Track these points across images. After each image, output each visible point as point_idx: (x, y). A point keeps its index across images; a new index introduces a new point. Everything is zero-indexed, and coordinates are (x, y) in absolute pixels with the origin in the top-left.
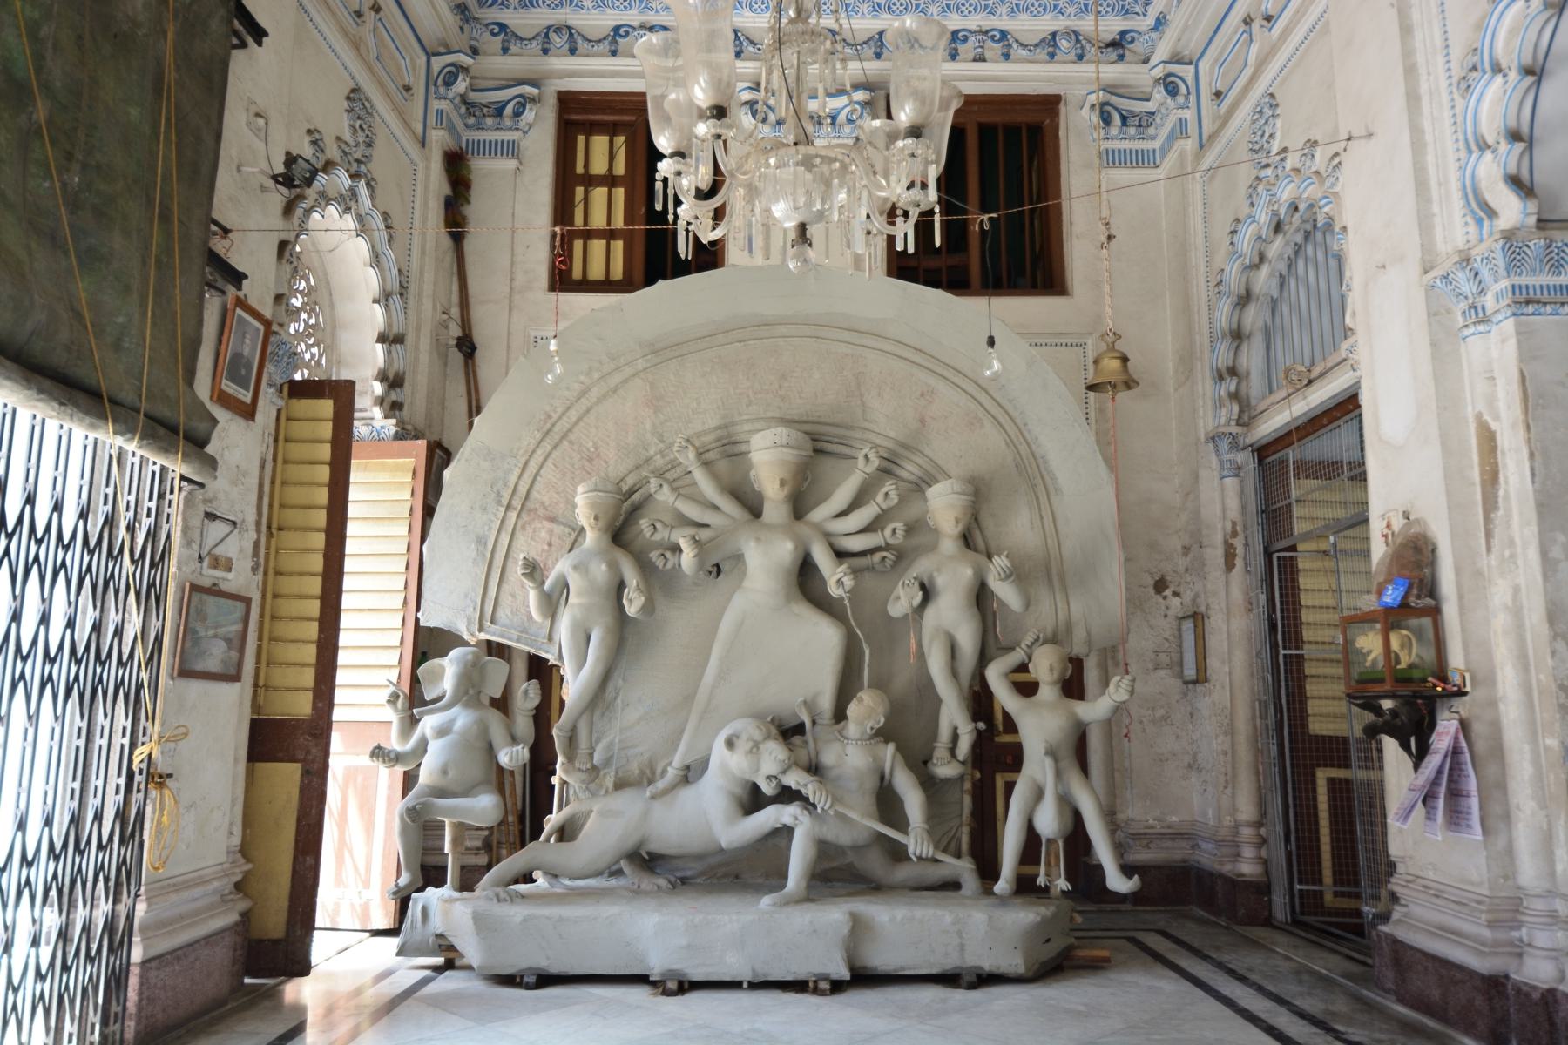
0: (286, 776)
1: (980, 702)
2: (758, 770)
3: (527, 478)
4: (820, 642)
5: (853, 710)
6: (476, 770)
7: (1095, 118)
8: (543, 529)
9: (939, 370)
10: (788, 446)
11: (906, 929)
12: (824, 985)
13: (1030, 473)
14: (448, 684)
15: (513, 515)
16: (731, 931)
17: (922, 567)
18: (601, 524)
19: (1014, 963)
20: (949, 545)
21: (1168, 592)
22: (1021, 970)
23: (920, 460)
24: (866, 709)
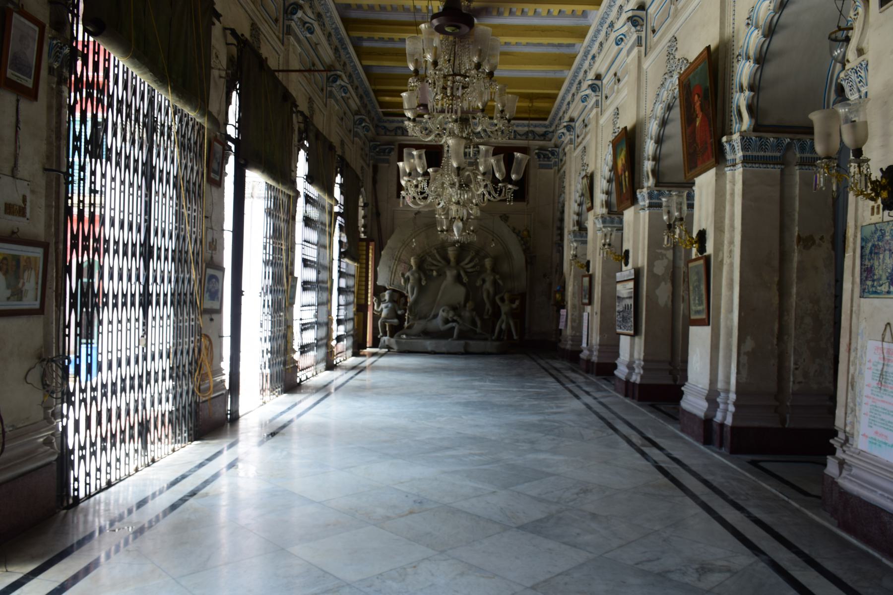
0: (361, 314)
1: (494, 304)
5: (468, 305)
8: (403, 265)
11: (474, 345)
14: (387, 297)
16: (443, 345)
20: (489, 272)
24: (470, 305)
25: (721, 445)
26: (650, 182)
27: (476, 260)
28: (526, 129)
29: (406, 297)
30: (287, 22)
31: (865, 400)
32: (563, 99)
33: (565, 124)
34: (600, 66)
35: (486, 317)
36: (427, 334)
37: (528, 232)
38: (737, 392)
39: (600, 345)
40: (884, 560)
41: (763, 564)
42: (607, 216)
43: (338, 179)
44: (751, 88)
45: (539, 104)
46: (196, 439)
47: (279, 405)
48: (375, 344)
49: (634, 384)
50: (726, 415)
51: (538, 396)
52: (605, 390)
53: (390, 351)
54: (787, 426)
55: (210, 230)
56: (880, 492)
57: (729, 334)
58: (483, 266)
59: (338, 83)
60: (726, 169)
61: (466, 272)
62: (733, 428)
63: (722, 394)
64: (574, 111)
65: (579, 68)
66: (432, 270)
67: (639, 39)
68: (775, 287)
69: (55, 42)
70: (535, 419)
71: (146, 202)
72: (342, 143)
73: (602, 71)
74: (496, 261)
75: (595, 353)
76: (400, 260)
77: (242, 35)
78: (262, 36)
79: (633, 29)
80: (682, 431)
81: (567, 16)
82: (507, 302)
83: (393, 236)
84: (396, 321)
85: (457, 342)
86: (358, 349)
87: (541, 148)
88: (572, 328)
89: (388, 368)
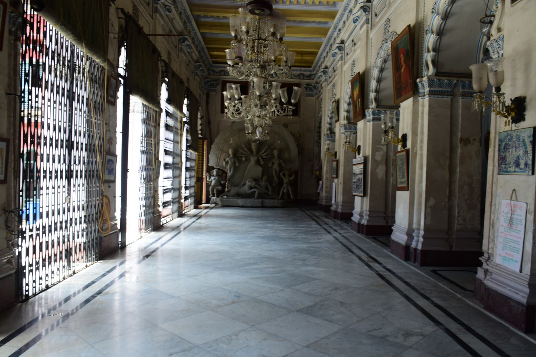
0: (199, 183)
1: (279, 177)
8: (225, 154)
11: (267, 202)
16: (249, 202)
20: (276, 158)
24: (265, 178)
25: (415, 261)
26: (373, 105)
27: (269, 151)
28: (299, 72)
29: (226, 173)
30: (155, 5)
31: (500, 234)
32: (321, 55)
33: (322, 70)
34: (344, 35)
35: (274, 185)
36: (239, 195)
37: (300, 134)
38: (425, 230)
39: (343, 202)
40: (511, 328)
41: (441, 331)
42: (347, 125)
43: (186, 101)
44: (434, 50)
45: (307, 58)
46: (100, 260)
47: (150, 238)
48: (208, 201)
49: (363, 225)
50: (418, 243)
51: (306, 233)
52: (346, 229)
53: (216, 206)
54: (453, 250)
55: (108, 132)
56: (509, 288)
57: (420, 196)
58: (273, 155)
59: (186, 43)
60: (419, 98)
61: (263, 158)
62: (422, 251)
63: (416, 231)
64: (328, 62)
65: (331, 36)
66: (242, 157)
67: (367, 19)
68: (447, 168)
69: (13, 15)
70: (304, 246)
71: (69, 114)
72: (188, 79)
73: (345, 38)
74: (280, 151)
75: (340, 207)
76: (222, 151)
77: (128, 12)
78: (140, 13)
79: (364, 14)
80: (392, 253)
81: (324, 5)
82: (287, 176)
83: (219, 136)
84: (220, 187)
86: (197, 204)
87: (308, 84)
88: (326, 192)
89: (216, 216)
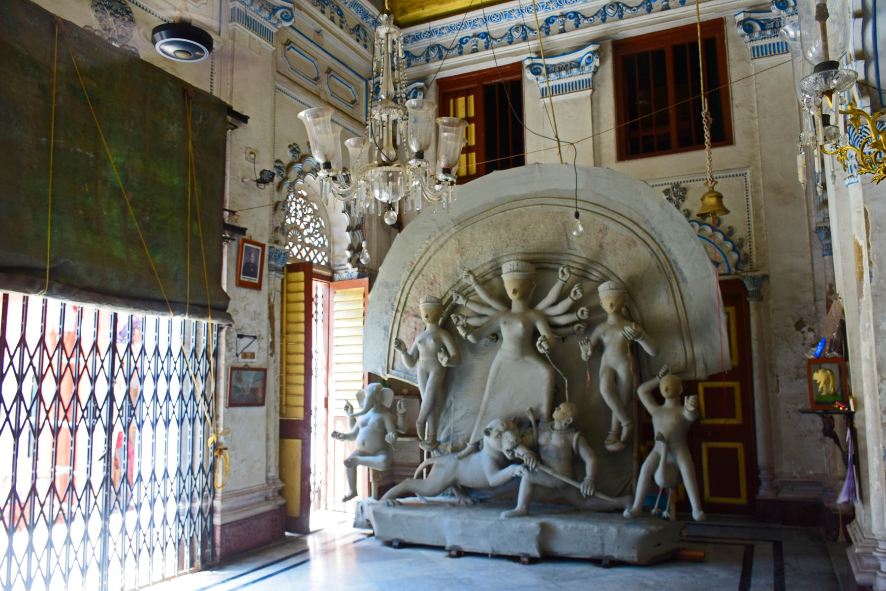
2: (501, 447)
3: (404, 295)
4: (539, 376)
5: (556, 415)
6: (378, 445)
7: (741, 31)
9: (609, 214)
10: (517, 271)
11: (570, 533)
12: (525, 559)
13: (667, 271)
15: (399, 315)
17: (598, 331)
18: (429, 319)
19: (632, 555)
20: (611, 319)
21: (805, 329)
22: (636, 560)
23: (600, 269)
24: (562, 415)
27: (576, 293)
35: (611, 447)
37: (719, 197)
61: (553, 327)
82: (668, 403)
85: (516, 524)
